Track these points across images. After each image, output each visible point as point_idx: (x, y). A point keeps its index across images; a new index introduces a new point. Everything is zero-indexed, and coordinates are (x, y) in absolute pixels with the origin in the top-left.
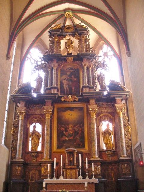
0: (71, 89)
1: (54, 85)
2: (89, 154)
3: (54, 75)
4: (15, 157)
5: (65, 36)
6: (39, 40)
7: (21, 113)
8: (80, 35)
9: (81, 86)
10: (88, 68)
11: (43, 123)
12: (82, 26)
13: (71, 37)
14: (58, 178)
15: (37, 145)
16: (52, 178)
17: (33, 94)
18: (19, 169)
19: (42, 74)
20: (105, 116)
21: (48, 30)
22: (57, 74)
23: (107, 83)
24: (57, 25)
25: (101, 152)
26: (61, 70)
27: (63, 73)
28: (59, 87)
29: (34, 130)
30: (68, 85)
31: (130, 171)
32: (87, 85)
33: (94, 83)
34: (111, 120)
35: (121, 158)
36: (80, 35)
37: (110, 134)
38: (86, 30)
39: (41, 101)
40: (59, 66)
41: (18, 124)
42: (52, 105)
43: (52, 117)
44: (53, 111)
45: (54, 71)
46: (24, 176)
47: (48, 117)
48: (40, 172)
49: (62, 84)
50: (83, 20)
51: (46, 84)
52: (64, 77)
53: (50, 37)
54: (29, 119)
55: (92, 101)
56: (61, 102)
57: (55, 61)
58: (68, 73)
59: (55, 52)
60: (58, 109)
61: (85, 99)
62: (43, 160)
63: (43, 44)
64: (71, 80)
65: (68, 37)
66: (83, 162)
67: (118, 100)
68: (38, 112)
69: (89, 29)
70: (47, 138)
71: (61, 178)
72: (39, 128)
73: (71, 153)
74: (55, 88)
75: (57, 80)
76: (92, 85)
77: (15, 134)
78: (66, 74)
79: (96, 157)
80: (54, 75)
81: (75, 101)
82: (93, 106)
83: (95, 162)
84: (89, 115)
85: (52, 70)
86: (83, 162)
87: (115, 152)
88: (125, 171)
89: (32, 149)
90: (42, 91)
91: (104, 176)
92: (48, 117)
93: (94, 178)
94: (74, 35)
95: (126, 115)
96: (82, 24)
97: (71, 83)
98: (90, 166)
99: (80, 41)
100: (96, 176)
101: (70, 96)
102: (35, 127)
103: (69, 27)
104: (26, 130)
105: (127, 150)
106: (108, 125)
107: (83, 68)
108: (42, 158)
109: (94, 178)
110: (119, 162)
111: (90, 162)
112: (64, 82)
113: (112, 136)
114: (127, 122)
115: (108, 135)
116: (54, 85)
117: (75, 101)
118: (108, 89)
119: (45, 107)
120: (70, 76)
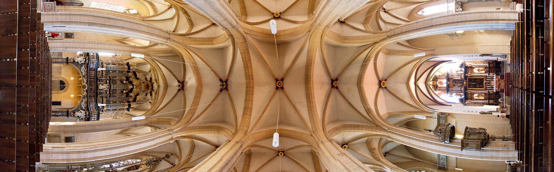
0: (461, 83)
1: (460, 89)
2: (486, 77)
3: (455, 89)
4: (487, 103)
5: (437, 85)
6: (439, 95)
7: (470, 101)
8: (437, 78)
9: (460, 79)
10: (452, 76)
11: (474, 94)
12: (434, 78)
13: (437, 82)
14: (494, 88)
15: (482, 95)
16: (494, 90)
17: (462, 98)
18: (491, 101)
19: (454, 94)
20: (472, 70)
21: (434, 91)
22: (454, 88)
23: (459, 69)
24: (433, 88)
25: (486, 73)
26: (453, 86)
27: (454, 86)
28: (461, 87)
29: (477, 97)
30: (459, 84)
31: (492, 63)
32: (460, 77)
33: (459, 74)
34: (474, 68)
35: (488, 66)
36: (437, 78)
37: (479, 69)
38: (435, 76)
39: (466, 94)
40: (451, 87)
41: (474, 102)
42: (467, 90)
43: (472, 90)
44: (469, 89)
45: (453, 89)
46: (493, 99)
47: (472, 91)
48: (492, 94)
49: (458, 86)
50: (431, 77)
51: (458, 92)
52: (456, 85)
53: (437, 91)
54: (472, 99)
55: (467, 75)
56: (466, 87)
57: (449, 89)
58: (454, 84)
59: (445, 89)
60: (469, 87)
61: (466, 77)
62: (488, 93)
63: (439, 93)
64: (457, 83)
65: (438, 84)
66: (489, 79)
67: (466, 66)
68: (470, 95)
69: (434, 75)
70: (480, 92)
71: (494, 87)
72: (475, 95)
73: (486, 83)
74: (461, 89)
75: (457, 88)
76: (460, 75)
77: (478, 103)
78: (455, 85)
79: (487, 74)
80: (455, 89)
81: (467, 81)
82: (468, 75)
83: (489, 75)
84: (471, 76)
85: (452, 90)
86: (489, 79)
87: (486, 68)
88: (492, 65)
89: (484, 97)
90: (461, 94)
91: (494, 72)
92: (472, 91)
93: (494, 76)
94: (437, 81)
95: (472, 63)
96: (433, 77)
97: (459, 83)
98: (490, 77)
99: (439, 78)
100: (493, 75)
101: (464, 83)
102: (475, 96)
103: (433, 83)
104: (476, 99)
105: (485, 64)
106: (476, 70)
107: (452, 78)
108: (487, 93)
109: (494, 76)
110: (489, 67)
111: (489, 77)
112: (458, 85)
113: (479, 68)
114: (475, 63)
115: (479, 70)
116: (460, 89)
117: (467, 81)
118: (461, 69)
119: (468, 92)
120: (456, 83)
